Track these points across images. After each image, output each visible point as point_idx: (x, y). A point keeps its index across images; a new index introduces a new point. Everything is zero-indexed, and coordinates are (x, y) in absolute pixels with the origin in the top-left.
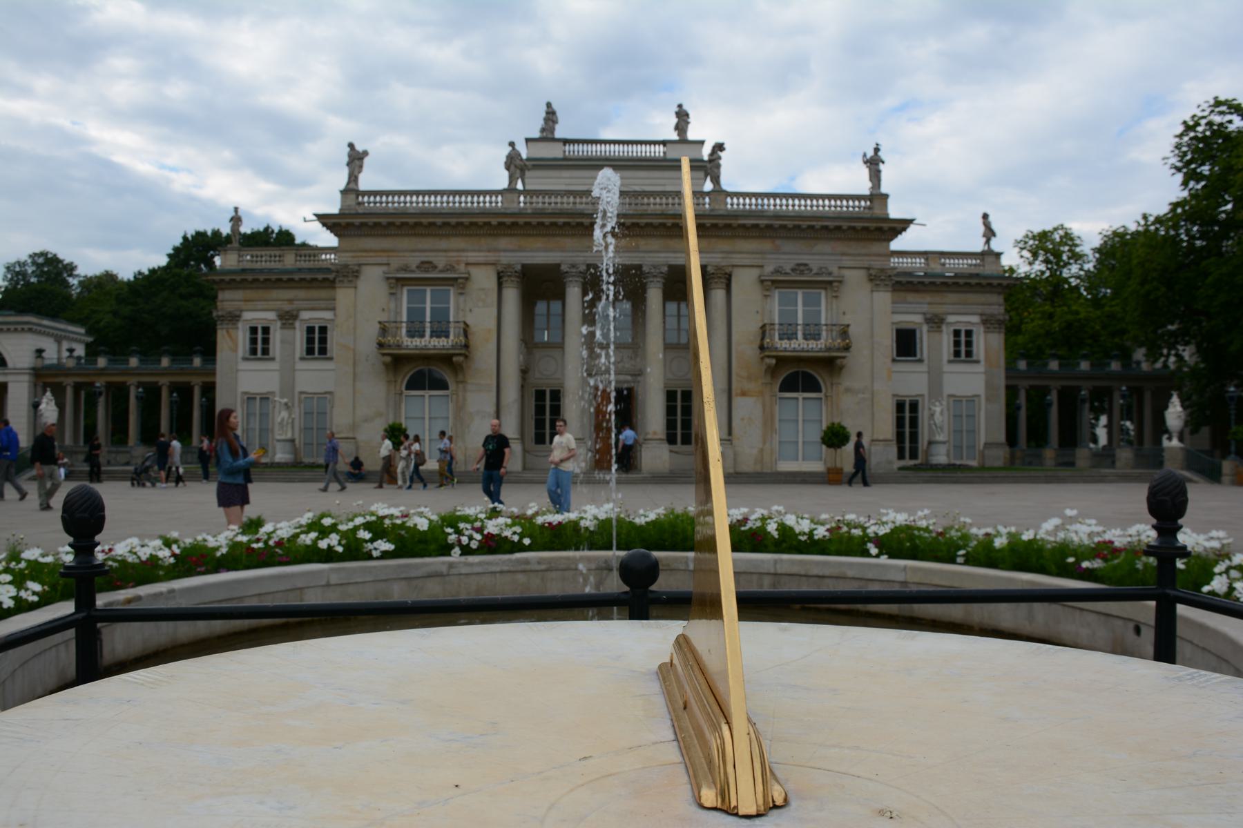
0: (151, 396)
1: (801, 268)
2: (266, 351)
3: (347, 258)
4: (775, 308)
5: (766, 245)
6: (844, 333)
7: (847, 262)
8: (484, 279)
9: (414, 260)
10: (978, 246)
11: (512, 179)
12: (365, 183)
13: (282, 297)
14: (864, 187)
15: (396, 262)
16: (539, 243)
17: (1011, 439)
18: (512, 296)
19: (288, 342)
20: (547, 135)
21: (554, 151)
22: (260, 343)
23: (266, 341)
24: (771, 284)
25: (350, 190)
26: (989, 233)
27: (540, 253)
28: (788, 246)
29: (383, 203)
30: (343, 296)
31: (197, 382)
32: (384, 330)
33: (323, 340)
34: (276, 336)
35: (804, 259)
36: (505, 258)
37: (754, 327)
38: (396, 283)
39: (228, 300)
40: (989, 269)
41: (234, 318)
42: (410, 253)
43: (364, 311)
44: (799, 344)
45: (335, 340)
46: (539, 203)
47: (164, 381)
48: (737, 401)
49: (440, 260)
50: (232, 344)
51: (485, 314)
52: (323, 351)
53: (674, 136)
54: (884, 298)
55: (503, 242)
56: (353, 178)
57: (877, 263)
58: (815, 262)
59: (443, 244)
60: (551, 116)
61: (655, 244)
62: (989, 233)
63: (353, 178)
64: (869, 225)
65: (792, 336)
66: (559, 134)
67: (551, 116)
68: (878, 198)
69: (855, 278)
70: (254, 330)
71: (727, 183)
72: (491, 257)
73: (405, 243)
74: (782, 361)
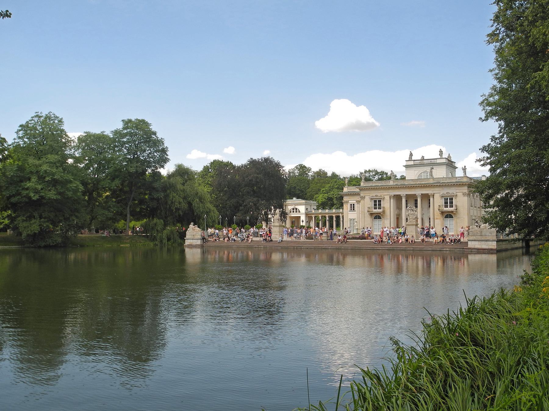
0: (331, 218)
2: (354, 209)
5: (440, 189)
6: (456, 206)
7: (458, 191)
8: (387, 198)
15: (371, 195)
16: (397, 191)
18: (392, 200)
20: (410, 159)
21: (412, 163)
22: (353, 207)
23: (354, 207)
27: (397, 193)
28: (445, 189)
31: (341, 215)
34: (356, 206)
39: (345, 199)
41: (347, 202)
49: (379, 195)
50: (346, 207)
53: (439, 157)
55: (390, 191)
59: (379, 192)
60: (411, 155)
61: (418, 190)
66: (413, 158)
67: (411, 155)
69: (460, 195)
70: (351, 205)
72: (388, 194)
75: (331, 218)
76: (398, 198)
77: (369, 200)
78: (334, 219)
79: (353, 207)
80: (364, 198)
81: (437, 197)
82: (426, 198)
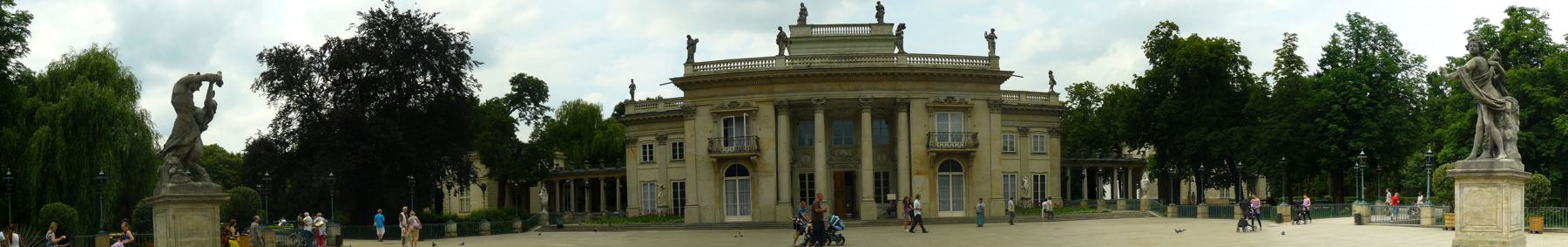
1: (950, 99)
3: (688, 103)
4: (936, 125)
6: (975, 136)
8: (767, 111)
9: (727, 101)
10: (1047, 90)
11: (781, 50)
12: (698, 58)
13: (659, 129)
14: (985, 52)
15: (717, 103)
17: (1064, 196)
19: (662, 153)
22: (648, 156)
24: (932, 109)
25: (690, 61)
26: (1053, 82)
27: (799, 95)
29: (712, 69)
30: (688, 125)
32: (711, 142)
33: (681, 151)
34: (657, 149)
35: (952, 94)
36: (779, 98)
37: (924, 136)
38: (716, 115)
40: (1052, 102)
41: (634, 141)
42: (724, 99)
43: (701, 132)
44: (949, 144)
45: (687, 150)
46: (799, 64)
47: (601, 177)
48: (915, 178)
49: (741, 100)
50: (634, 157)
51: (769, 133)
52: (682, 156)
54: (997, 118)
55: (778, 88)
56: (691, 56)
57: (995, 97)
58: (958, 96)
59: (742, 90)
62: (1053, 82)
63: (691, 56)
64: (986, 74)
65: (946, 139)
68: (993, 58)
69: (981, 106)
71: (907, 49)
72: (770, 97)
73: (720, 91)
74: (940, 154)
75: (595, 184)
76: (799, 115)
77: (709, 119)
78: (602, 184)
79: (648, 156)
80: (694, 112)
81: (917, 107)
82: (887, 114)
